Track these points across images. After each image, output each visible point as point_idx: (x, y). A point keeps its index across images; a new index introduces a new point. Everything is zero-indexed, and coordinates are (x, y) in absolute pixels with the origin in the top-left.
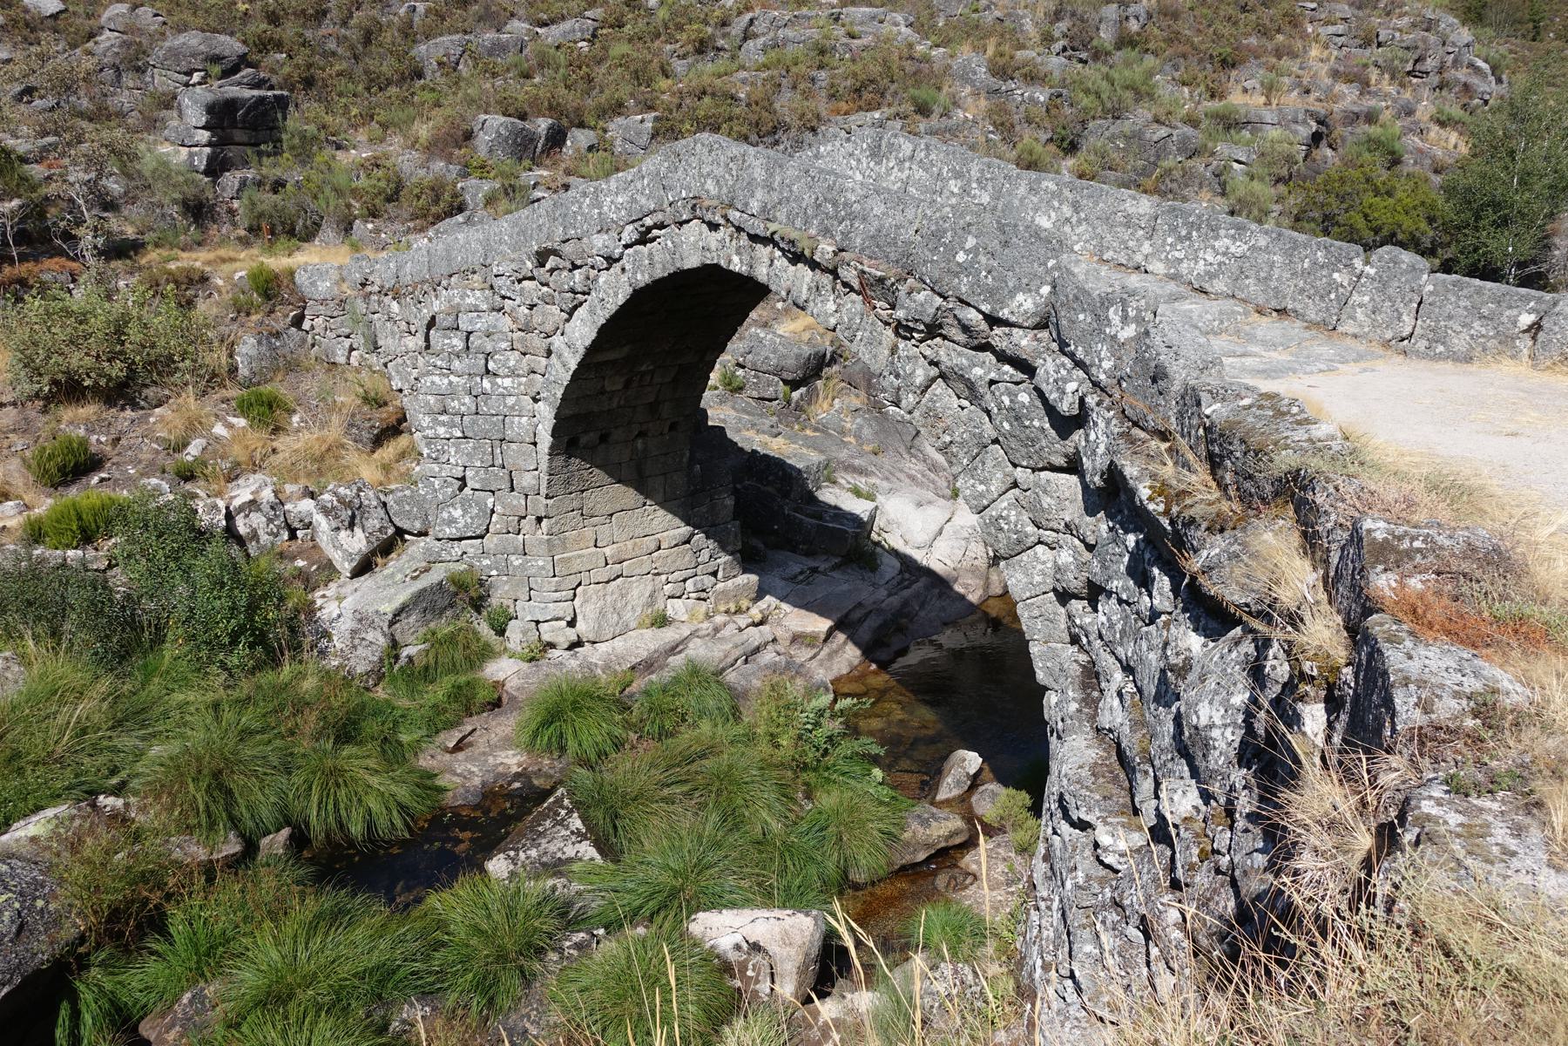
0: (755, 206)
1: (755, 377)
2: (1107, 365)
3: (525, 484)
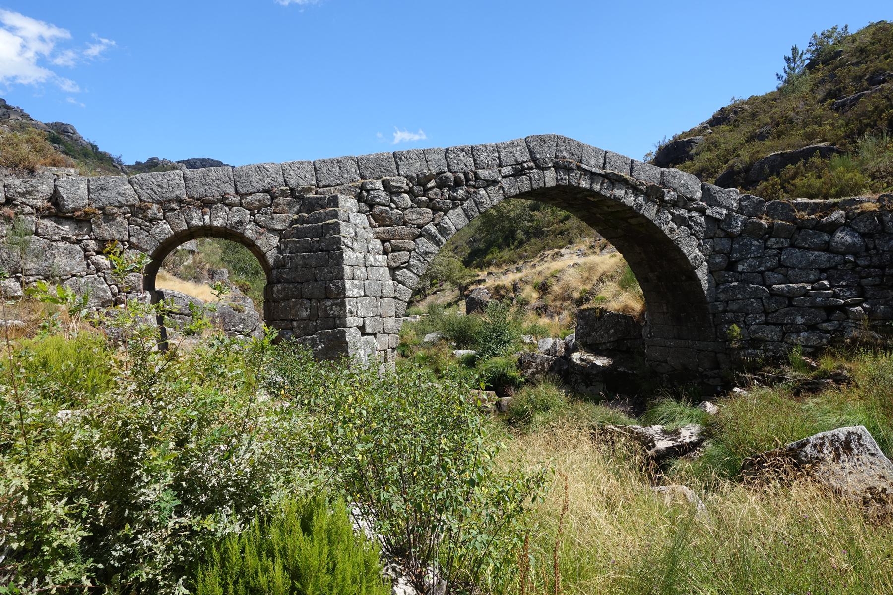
0: (593, 162)
1: (180, 319)
2: (735, 205)
3: (389, 326)
